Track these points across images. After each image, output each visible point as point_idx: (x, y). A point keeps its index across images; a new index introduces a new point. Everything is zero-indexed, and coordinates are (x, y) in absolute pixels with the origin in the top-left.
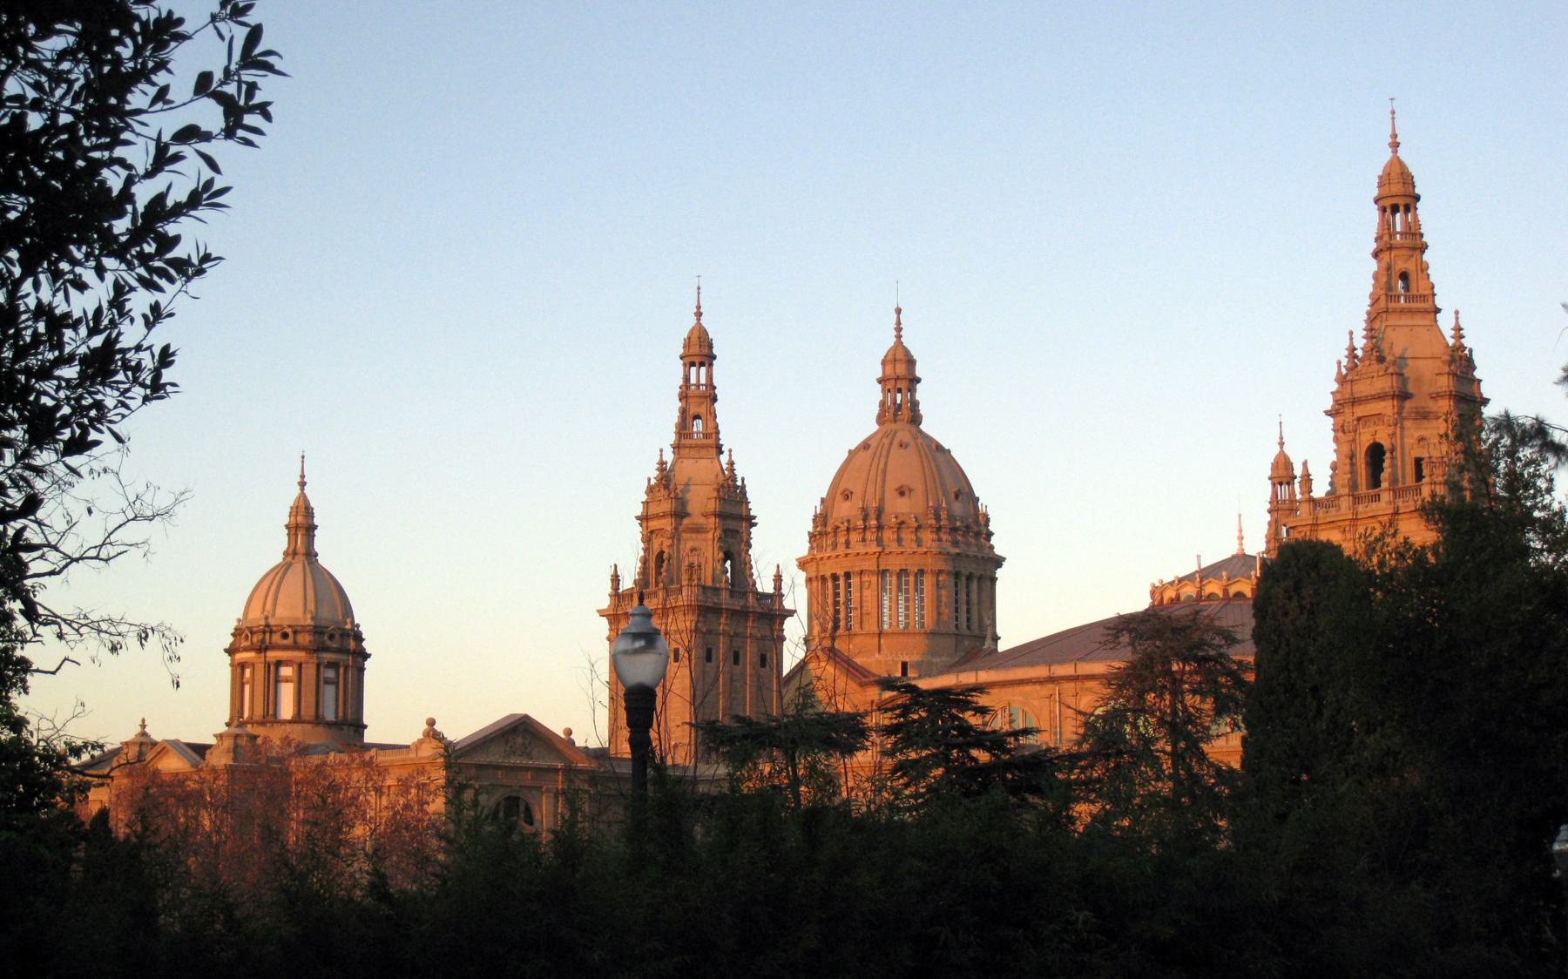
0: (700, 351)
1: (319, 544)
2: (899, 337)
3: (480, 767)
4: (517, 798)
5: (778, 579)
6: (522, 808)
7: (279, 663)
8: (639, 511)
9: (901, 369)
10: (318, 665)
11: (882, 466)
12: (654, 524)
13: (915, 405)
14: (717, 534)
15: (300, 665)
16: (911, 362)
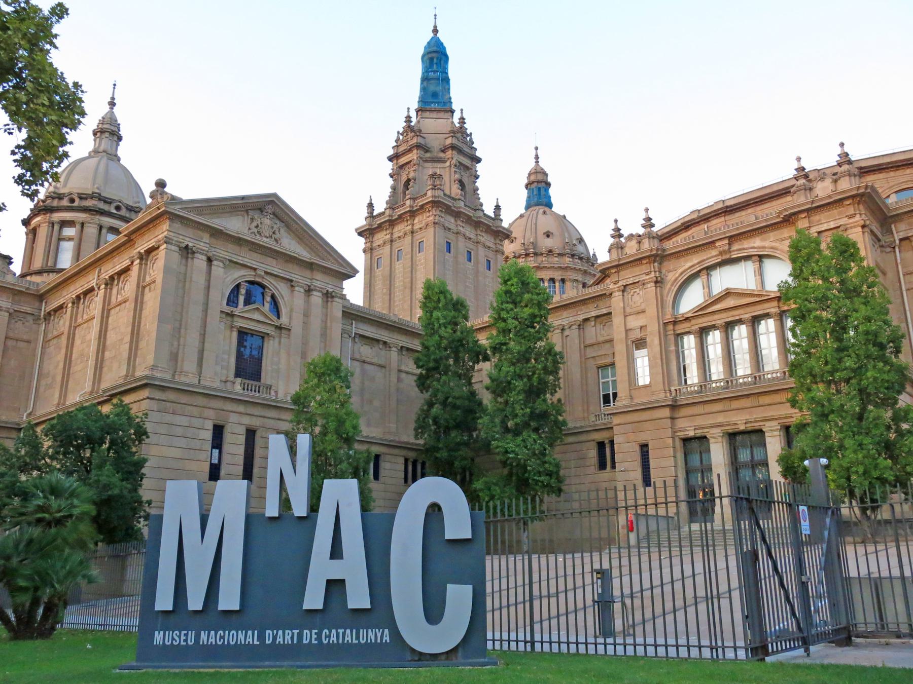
0: (436, 58)
1: (123, 150)
2: (537, 162)
3: (217, 234)
4: (263, 287)
5: (498, 208)
6: (268, 299)
7: (64, 224)
8: (391, 152)
9: (540, 177)
10: (101, 228)
11: (534, 221)
12: (403, 160)
13: (550, 197)
14: (454, 162)
15: (83, 224)
16: (546, 175)
